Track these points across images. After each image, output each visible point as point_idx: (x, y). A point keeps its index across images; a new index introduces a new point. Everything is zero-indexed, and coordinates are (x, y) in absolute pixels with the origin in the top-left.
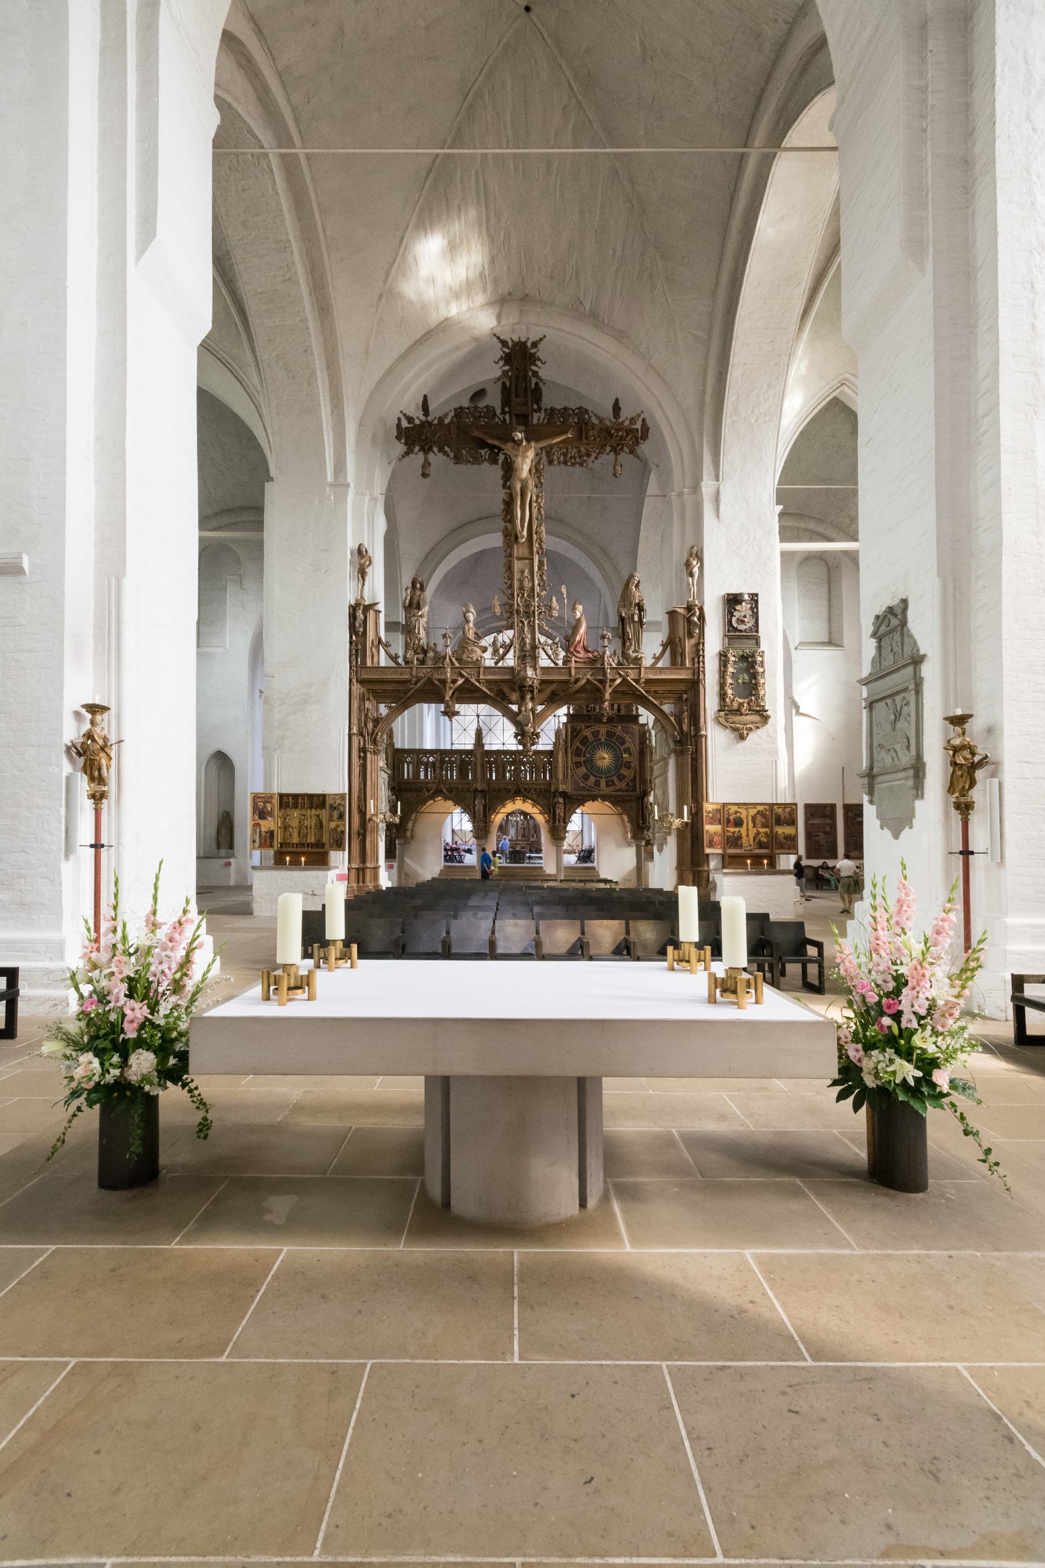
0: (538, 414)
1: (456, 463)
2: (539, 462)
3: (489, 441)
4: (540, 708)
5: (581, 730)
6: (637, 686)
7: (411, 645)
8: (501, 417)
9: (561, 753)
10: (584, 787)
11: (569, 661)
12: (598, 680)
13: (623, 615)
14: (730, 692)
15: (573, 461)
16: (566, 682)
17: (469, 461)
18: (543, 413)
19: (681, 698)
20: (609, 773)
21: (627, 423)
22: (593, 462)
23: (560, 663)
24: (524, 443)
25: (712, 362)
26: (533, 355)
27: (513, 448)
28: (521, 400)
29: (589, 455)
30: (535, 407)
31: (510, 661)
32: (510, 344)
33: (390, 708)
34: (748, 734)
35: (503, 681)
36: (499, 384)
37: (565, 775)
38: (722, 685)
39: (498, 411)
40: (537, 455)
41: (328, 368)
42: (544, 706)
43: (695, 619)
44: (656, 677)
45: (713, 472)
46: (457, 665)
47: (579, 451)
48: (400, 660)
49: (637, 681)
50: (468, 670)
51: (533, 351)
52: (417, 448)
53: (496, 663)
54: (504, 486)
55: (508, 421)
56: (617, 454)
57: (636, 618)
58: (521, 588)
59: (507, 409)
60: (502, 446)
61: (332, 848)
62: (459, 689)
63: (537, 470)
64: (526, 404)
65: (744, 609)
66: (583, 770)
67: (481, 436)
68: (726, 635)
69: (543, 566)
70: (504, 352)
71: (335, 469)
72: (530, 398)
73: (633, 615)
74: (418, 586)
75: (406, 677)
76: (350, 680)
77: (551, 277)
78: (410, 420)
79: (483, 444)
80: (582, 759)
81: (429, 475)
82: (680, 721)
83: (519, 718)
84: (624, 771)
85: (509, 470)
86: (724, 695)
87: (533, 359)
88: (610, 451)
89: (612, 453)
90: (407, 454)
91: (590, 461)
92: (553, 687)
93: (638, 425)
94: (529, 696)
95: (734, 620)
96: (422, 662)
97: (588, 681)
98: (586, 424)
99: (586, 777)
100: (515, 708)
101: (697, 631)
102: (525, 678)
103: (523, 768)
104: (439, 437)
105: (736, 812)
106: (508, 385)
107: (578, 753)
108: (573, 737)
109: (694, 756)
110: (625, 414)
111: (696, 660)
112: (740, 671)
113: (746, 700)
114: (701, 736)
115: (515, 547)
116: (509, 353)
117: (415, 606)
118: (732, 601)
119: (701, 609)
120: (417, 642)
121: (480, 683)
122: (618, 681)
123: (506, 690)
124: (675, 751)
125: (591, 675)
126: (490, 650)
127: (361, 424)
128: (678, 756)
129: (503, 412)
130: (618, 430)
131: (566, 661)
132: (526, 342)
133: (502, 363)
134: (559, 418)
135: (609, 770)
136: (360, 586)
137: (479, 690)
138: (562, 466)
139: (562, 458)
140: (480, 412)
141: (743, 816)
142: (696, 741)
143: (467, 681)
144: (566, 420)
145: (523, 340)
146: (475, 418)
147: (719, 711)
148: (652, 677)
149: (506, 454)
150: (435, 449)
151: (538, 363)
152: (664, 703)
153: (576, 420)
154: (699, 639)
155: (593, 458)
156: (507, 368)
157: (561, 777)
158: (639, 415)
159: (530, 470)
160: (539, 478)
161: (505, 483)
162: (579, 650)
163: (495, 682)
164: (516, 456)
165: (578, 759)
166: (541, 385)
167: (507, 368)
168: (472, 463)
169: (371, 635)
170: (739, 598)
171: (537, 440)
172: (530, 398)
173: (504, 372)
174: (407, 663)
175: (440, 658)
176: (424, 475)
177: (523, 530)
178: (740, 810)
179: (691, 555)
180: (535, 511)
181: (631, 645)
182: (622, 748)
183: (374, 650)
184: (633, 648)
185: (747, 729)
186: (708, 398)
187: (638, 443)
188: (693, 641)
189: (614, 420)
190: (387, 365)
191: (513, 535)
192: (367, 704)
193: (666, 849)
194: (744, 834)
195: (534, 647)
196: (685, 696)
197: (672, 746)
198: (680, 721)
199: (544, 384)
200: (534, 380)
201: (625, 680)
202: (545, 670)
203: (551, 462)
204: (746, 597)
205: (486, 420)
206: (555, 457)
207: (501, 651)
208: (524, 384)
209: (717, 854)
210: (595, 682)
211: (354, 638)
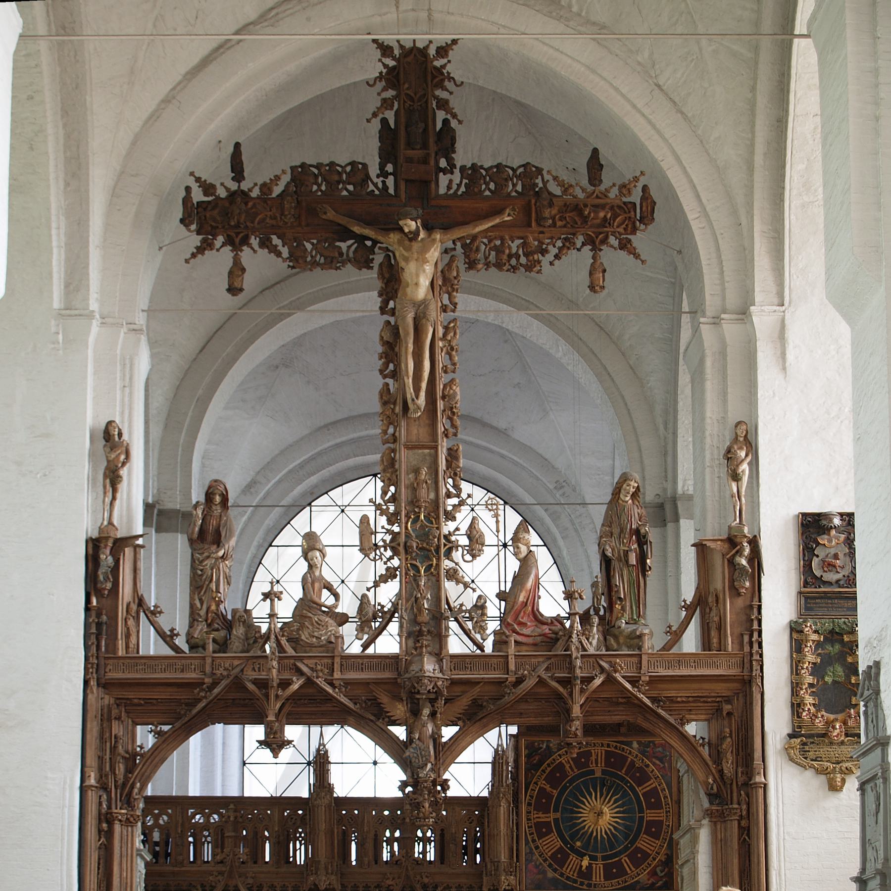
0: (449, 176)
1: (293, 267)
2: (449, 265)
3: (357, 229)
4: (448, 732)
5: (549, 752)
6: (634, 691)
7: (203, 613)
8: (379, 182)
9: (503, 804)
10: (554, 880)
12: (560, 681)
13: (609, 553)
14: (809, 700)
15: (513, 262)
16: (500, 683)
17: (318, 264)
18: (457, 172)
19: (719, 710)
20: (612, 847)
21: (613, 193)
22: (551, 263)
23: (488, 647)
24: (422, 235)
25: (762, 101)
26: (439, 70)
27: (400, 242)
28: (417, 153)
29: (544, 252)
30: (443, 163)
32: (397, 52)
33: (159, 734)
34: (843, 781)
35: (378, 683)
36: (376, 124)
37: (514, 853)
38: (795, 688)
39: (374, 171)
40: (446, 251)
41: (65, 113)
42: (455, 729)
43: (744, 562)
44: (670, 673)
45: (774, 289)
46: (290, 652)
48: (181, 642)
49: (634, 682)
50: (311, 662)
51: (438, 63)
52: (220, 239)
53: (365, 646)
54: (383, 310)
55: (391, 191)
56: (595, 249)
57: (633, 559)
58: (414, 502)
60: (380, 238)
62: (295, 698)
63: (445, 280)
64: (425, 161)
65: (831, 543)
66: (553, 842)
67: (343, 221)
68: (800, 593)
69: (457, 458)
70: (385, 66)
71: (67, 285)
72: (433, 148)
73: (626, 553)
74: (218, 499)
75: (192, 675)
76: (86, 683)
78: (208, 188)
79: (345, 234)
80: (551, 817)
81: (241, 290)
82: (717, 756)
83: (407, 754)
84: (644, 843)
86: (799, 705)
87: (439, 77)
88: (583, 244)
90: (200, 250)
91: (546, 260)
92: (476, 691)
93: (636, 197)
94: (426, 711)
95: (815, 563)
96: (223, 646)
97: (541, 682)
98: (537, 194)
99: (559, 858)
100: (400, 732)
101: (747, 584)
102: (419, 680)
103: (419, 834)
104: (263, 220)
106: (393, 127)
107: (542, 803)
108: (532, 768)
109: (744, 823)
110: (607, 179)
111: (746, 638)
113: (840, 716)
114: (757, 785)
115: (403, 423)
116: (394, 68)
117: (210, 538)
119: (754, 543)
120: (213, 607)
121: (331, 684)
122: (598, 681)
123: (384, 699)
124: (708, 813)
125: (547, 669)
127: (115, 194)
128: (715, 823)
129: (383, 174)
130: (597, 207)
131: (500, 642)
133: (380, 85)
134: (487, 184)
135: (611, 840)
136: (108, 500)
137: (330, 698)
138: (493, 270)
140: (340, 174)
142: (748, 795)
143: (309, 682)
144: (500, 187)
145: (420, 45)
146: (328, 183)
147: (791, 736)
148: (663, 672)
149: (387, 249)
150: (254, 241)
151: (448, 84)
152: (689, 722)
153: (519, 188)
155: (550, 257)
156: (390, 93)
157: (504, 858)
158: (636, 179)
159: (432, 284)
161: (385, 303)
162: (524, 620)
163: (366, 684)
164: (407, 260)
165: (543, 817)
166: (454, 124)
167: (390, 93)
168: (323, 267)
170: (824, 522)
171: (446, 228)
172: (433, 148)
173: (384, 101)
174: (192, 647)
175: (255, 638)
176: (233, 290)
180: (442, 359)
181: (623, 609)
182: (640, 791)
183: (131, 622)
184: (627, 616)
185: (841, 772)
186: (759, 159)
187: (634, 231)
188: (740, 602)
189: (590, 188)
190: (164, 89)
191: (399, 402)
192: (117, 729)
195: (438, 618)
196: (727, 708)
197: (706, 804)
198: (717, 756)
199: (460, 122)
200: (441, 115)
201: (610, 680)
202: (460, 660)
203: (471, 265)
204: (837, 521)
205: (351, 188)
206: (480, 256)
208: (423, 125)
210: (554, 684)
211: (94, 602)
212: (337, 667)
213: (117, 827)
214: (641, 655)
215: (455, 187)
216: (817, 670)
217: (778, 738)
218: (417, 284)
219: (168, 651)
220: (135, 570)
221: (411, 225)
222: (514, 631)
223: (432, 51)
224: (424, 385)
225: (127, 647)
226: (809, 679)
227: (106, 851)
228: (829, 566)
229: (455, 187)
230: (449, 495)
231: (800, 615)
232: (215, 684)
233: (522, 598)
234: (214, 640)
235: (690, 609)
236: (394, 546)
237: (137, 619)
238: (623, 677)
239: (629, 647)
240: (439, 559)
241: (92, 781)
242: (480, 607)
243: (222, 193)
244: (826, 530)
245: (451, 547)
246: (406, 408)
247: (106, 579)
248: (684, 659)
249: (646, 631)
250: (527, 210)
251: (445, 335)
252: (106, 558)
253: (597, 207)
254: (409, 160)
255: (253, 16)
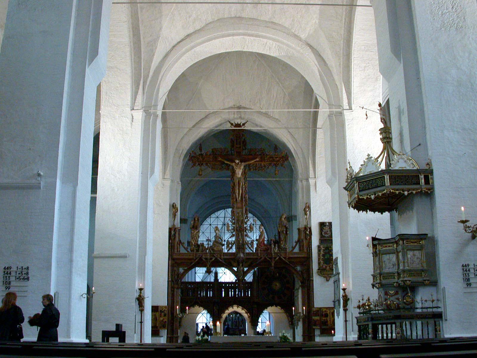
0: (245, 151)
3: (226, 162)
4: (246, 269)
7: (194, 243)
11: (258, 250)
13: (280, 230)
15: (259, 169)
16: (257, 258)
18: (247, 150)
23: (254, 251)
30: (244, 148)
31: (234, 250)
34: (329, 279)
38: (319, 259)
42: (247, 268)
46: (212, 252)
47: (261, 165)
49: (285, 258)
53: (228, 251)
57: (285, 232)
58: (238, 220)
59: (233, 149)
61: (161, 327)
63: (245, 173)
64: (240, 147)
65: (326, 229)
68: (320, 239)
75: (191, 257)
76: (169, 258)
77: (250, 101)
78: (195, 154)
85: (234, 172)
89: (274, 166)
94: (241, 265)
95: (323, 233)
96: (198, 251)
100: (235, 269)
101: (309, 237)
105: (325, 311)
112: (326, 253)
113: (329, 265)
118: (322, 225)
119: (310, 228)
120: (196, 242)
121: (221, 259)
122: (277, 258)
123: (232, 262)
125: (266, 256)
126: (226, 246)
130: (276, 158)
132: (240, 124)
137: (220, 262)
139: (254, 168)
141: (328, 312)
143: (216, 259)
145: (239, 123)
147: (318, 270)
153: (260, 153)
154: (310, 240)
155: (267, 168)
160: (245, 176)
169: (177, 239)
170: (325, 224)
171: (245, 162)
174: (191, 251)
177: (239, 197)
178: (327, 310)
179: (306, 207)
180: (244, 189)
192: (175, 269)
193: (299, 327)
194: (329, 320)
196: (305, 263)
201: (280, 258)
202: (249, 254)
203: (250, 169)
204: (327, 224)
206: (252, 168)
207: (230, 246)
209: (318, 329)
210: (268, 259)
211: (170, 241)
212: (222, 255)
213: (175, 290)
214: (286, 253)
215: (246, 153)
216: (323, 255)
217: (315, 271)
218: (239, 174)
219: (186, 252)
220: (179, 234)
221: (237, 161)
222: (259, 247)
223: (241, 124)
224: (240, 195)
225: (177, 251)
226: (322, 257)
227: (173, 295)
228: (326, 233)
229: (246, 153)
230: (246, 219)
231: (320, 244)
232: (196, 259)
233: (261, 240)
234: (196, 250)
235: (296, 243)
236: (234, 229)
237: (179, 245)
238: (283, 257)
239: (284, 251)
240: (243, 232)
241: (170, 280)
242: (252, 242)
243: (197, 154)
244: (325, 226)
245: (246, 229)
246: (236, 200)
247: (173, 236)
248: (295, 253)
249: (287, 247)
250: (261, 158)
251: (244, 184)
252: (173, 233)
253: (276, 158)
254: (237, 147)
255: (204, 117)
